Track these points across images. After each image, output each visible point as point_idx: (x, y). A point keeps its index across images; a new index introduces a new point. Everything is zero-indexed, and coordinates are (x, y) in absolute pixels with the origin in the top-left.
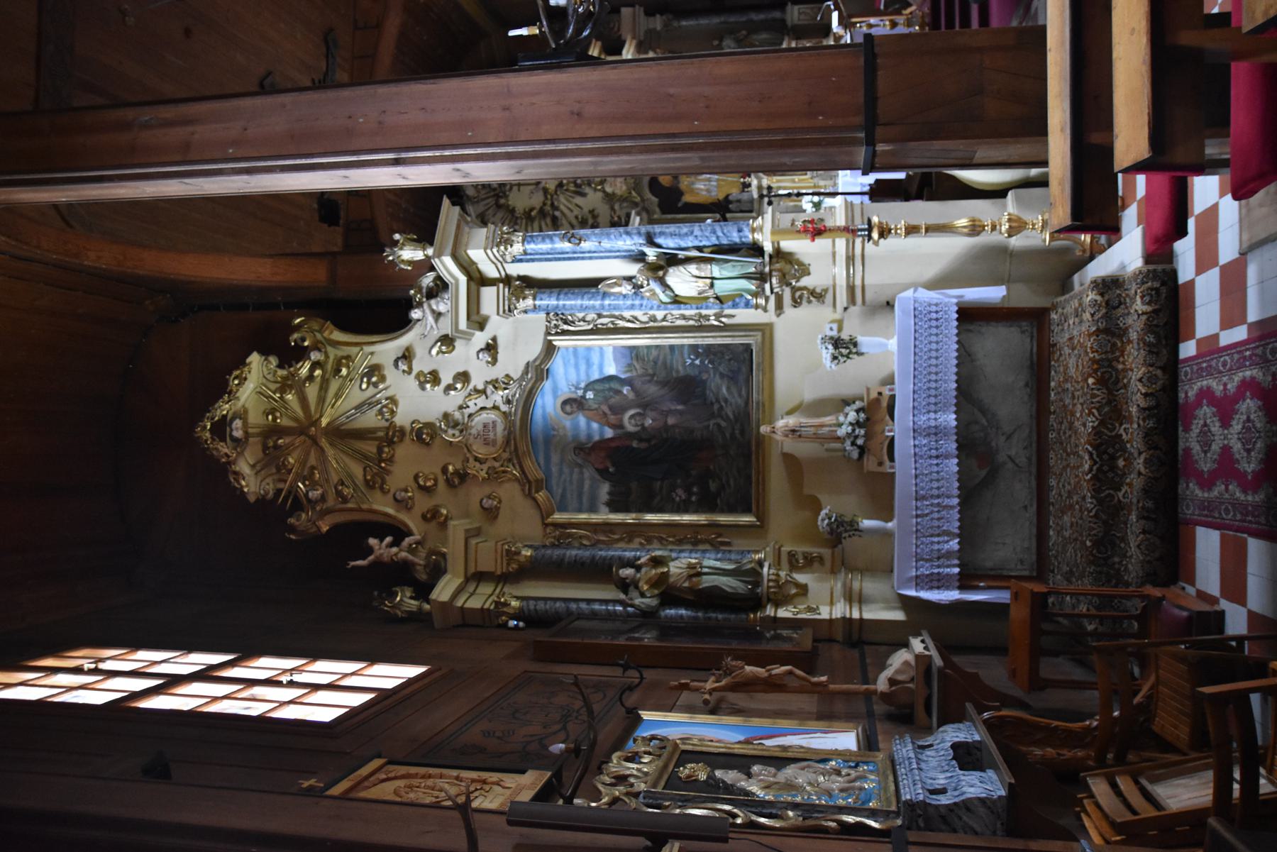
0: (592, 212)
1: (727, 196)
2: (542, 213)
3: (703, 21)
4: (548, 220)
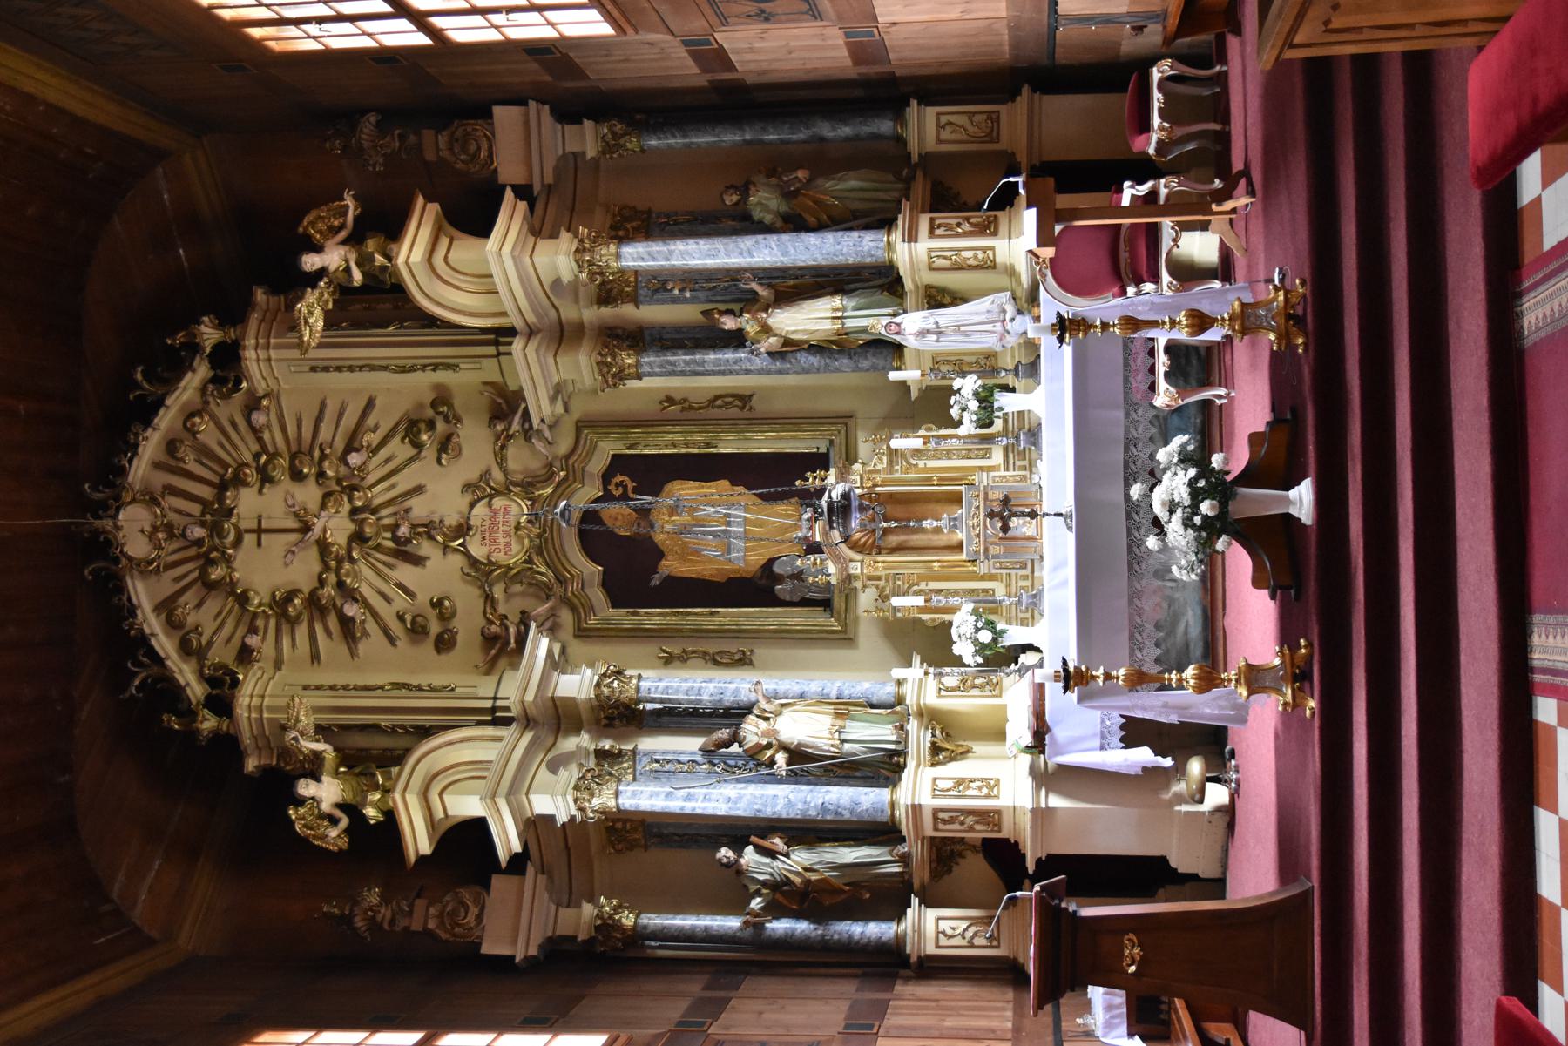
0: (437, 604)
1: (771, 561)
2: (314, 603)
3: (703, 139)
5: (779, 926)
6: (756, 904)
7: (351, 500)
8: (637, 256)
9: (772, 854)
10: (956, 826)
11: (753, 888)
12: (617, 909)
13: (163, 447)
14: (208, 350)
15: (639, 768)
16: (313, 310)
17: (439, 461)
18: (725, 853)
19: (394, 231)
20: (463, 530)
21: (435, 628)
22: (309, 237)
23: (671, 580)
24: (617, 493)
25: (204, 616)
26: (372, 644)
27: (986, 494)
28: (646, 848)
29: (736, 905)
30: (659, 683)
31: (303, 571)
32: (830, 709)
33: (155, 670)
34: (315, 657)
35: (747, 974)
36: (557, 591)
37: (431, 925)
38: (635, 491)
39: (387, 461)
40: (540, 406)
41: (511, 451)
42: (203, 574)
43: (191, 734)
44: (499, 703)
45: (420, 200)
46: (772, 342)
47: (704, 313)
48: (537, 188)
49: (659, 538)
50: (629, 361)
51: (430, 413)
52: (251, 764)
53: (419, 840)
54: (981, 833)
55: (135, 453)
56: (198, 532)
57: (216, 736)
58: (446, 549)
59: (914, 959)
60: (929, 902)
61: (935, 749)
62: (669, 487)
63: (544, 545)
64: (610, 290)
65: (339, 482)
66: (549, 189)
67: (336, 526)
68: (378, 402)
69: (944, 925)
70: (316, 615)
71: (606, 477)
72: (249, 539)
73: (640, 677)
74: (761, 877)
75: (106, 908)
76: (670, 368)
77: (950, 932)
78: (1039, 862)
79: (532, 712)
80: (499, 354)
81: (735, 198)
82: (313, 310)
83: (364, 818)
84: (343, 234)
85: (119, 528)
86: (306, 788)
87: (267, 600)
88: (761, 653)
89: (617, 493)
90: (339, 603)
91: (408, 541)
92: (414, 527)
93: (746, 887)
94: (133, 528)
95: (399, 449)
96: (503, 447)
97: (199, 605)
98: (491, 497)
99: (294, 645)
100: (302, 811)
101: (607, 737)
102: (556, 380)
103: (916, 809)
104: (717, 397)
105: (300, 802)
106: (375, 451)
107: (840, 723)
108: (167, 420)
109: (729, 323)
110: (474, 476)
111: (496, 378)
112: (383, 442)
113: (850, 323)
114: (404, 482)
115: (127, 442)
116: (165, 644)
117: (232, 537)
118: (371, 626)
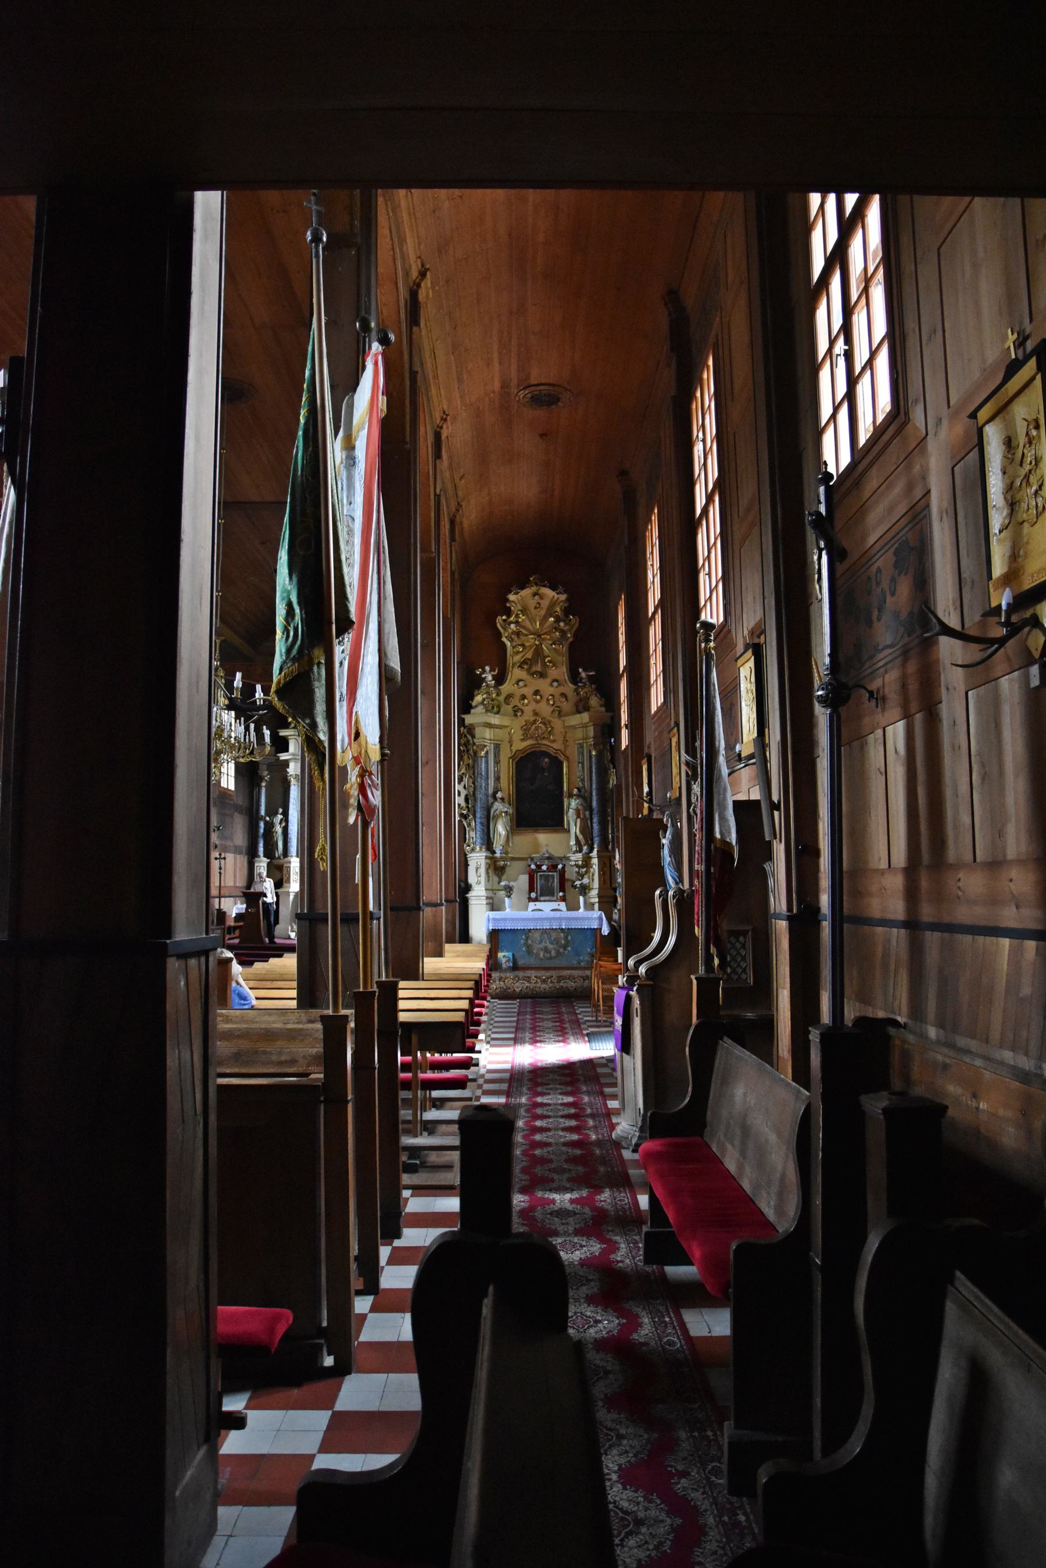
5: (262, 825)
6: (268, 819)
18: (281, 810)
29: (267, 813)
53: (283, 733)
60: (269, 864)
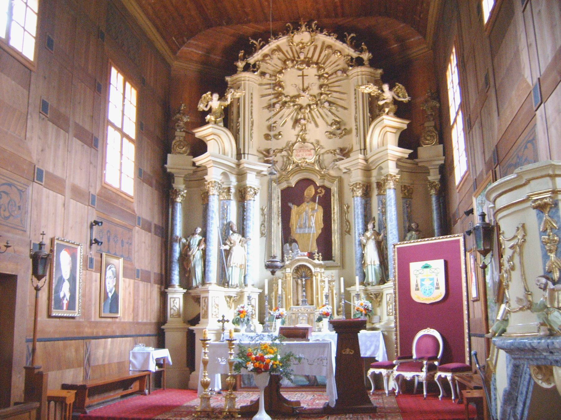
0: (280, 134)
4: (275, 100)
6: (184, 240)
7: (313, 104)
8: (391, 194)
9: (199, 245)
10: (204, 304)
11: (189, 239)
12: (182, 196)
13: (330, 44)
14: (361, 56)
15: (225, 201)
16: (371, 89)
17: (327, 132)
18: (199, 230)
19: (398, 114)
20: (304, 140)
21: (272, 133)
22: (395, 86)
23: (290, 209)
24: (319, 191)
25: (275, 62)
26: (267, 114)
27: (312, 313)
28: (203, 204)
30: (255, 207)
31: (290, 90)
32: (243, 263)
33: (258, 47)
34: (263, 96)
35: (162, 237)
36: (285, 173)
37: (177, 138)
38: (319, 196)
39: (327, 115)
40: (343, 164)
41: (330, 155)
42: (288, 59)
43: (237, 59)
44: (246, 155)
45: (407, 122)
46: (365, 241)
47: (374, 218)
48: (417, 160)
49: (304, 205)
50: (358, 193)
51: (343, 128)
52: (228, 79)
54: (202, 312)
55: (327, 35)
56: (302, 57)
57: (236, 67)
58: (298, 135)
59: (166, 290)
60: (186, 295)
61: (230, 297)
62: (321, 208)
63: (298, 168)
64: (380, 186)
65: (319, 100)
66: (417, 164)
67: (304, 100)
68: (346, 111)
69: (177, 300)
70: (276, 95)
71: (323, 187)
72: (300, 73)
73: (254, 200)
74: (191, 241)
75: (185, 39)
76: (356, 207)
77: (175, 302)
78: (193, 331)
79: (241, 167)
80: (361, 150)
81: (414, 227)
82: (371, 89)
83: (206, 116)
84: (396, 97)
85: (303, 32)
86: (216, 96)
87: (281, 80)
88: (264, 239)
89: (319, 191)
90: (280, 102)
91: (300, 123)
92: (305, 125)
93: (189, 237)
94: (303, 36)
95: (331, 118)
96: (331, 153)
97: (279, 59)
98: (315, 149)
99: (266, 89)
100: (210, 96)
101: (236, 191)
102: (352, 169)
103: (207, 291)
104: (349, 223)
105: (212, 95)
106: (330, 111)
107: (238, 266)
108: (339, 45)
109: (370, 226)
110: (322, 143)
111: (354, 150)
112: (333, 113)
113: (369, 267)
114: (320, 121)
115: (330, 33)
116: (266, 49)
117: (301, 67)
118: (273, 113)
